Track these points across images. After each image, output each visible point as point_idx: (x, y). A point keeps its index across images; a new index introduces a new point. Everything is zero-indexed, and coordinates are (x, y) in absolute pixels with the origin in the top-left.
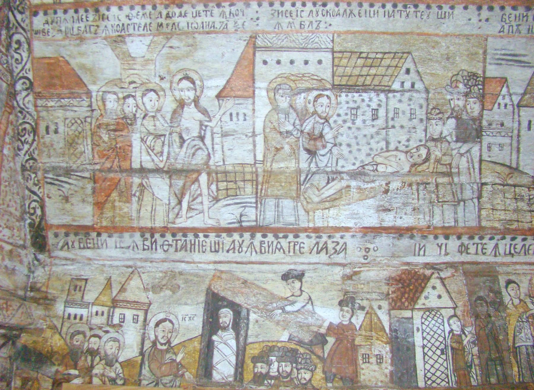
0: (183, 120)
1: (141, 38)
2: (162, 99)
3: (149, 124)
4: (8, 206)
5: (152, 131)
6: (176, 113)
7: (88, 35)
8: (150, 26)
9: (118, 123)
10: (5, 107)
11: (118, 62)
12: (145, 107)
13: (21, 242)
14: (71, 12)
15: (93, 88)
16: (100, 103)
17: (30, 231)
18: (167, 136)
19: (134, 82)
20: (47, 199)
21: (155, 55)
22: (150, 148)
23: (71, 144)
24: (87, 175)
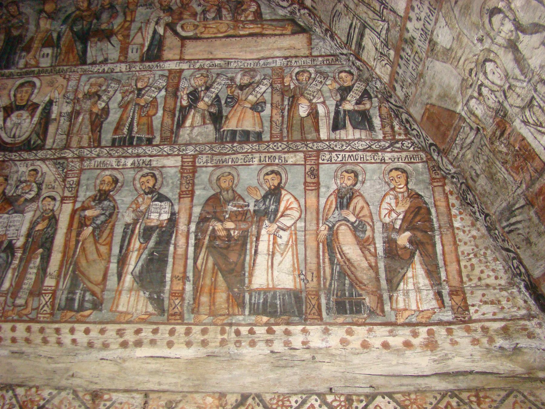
0: (530, 62)
1: (438, 25)
2: (498, 62)
3: (514, 100)
4: (480, 279)
5: (522, 105)
6: (519, 60)
7: (420, 68)
8: (432, 6)
9: (498, 124)
10: (431, 184)
11: (448, 65)
12: (496, 85)
13: (523, 312)
14: (402, 62)
15: (459, 109)
16: (473, 118)
17: (530, 295)
18: (535, 96)
19: (471, 70)
20: (518, 250)
21: (457, 26)
22: (537, 125)
23: (492, 178)
24: (522, 202)
